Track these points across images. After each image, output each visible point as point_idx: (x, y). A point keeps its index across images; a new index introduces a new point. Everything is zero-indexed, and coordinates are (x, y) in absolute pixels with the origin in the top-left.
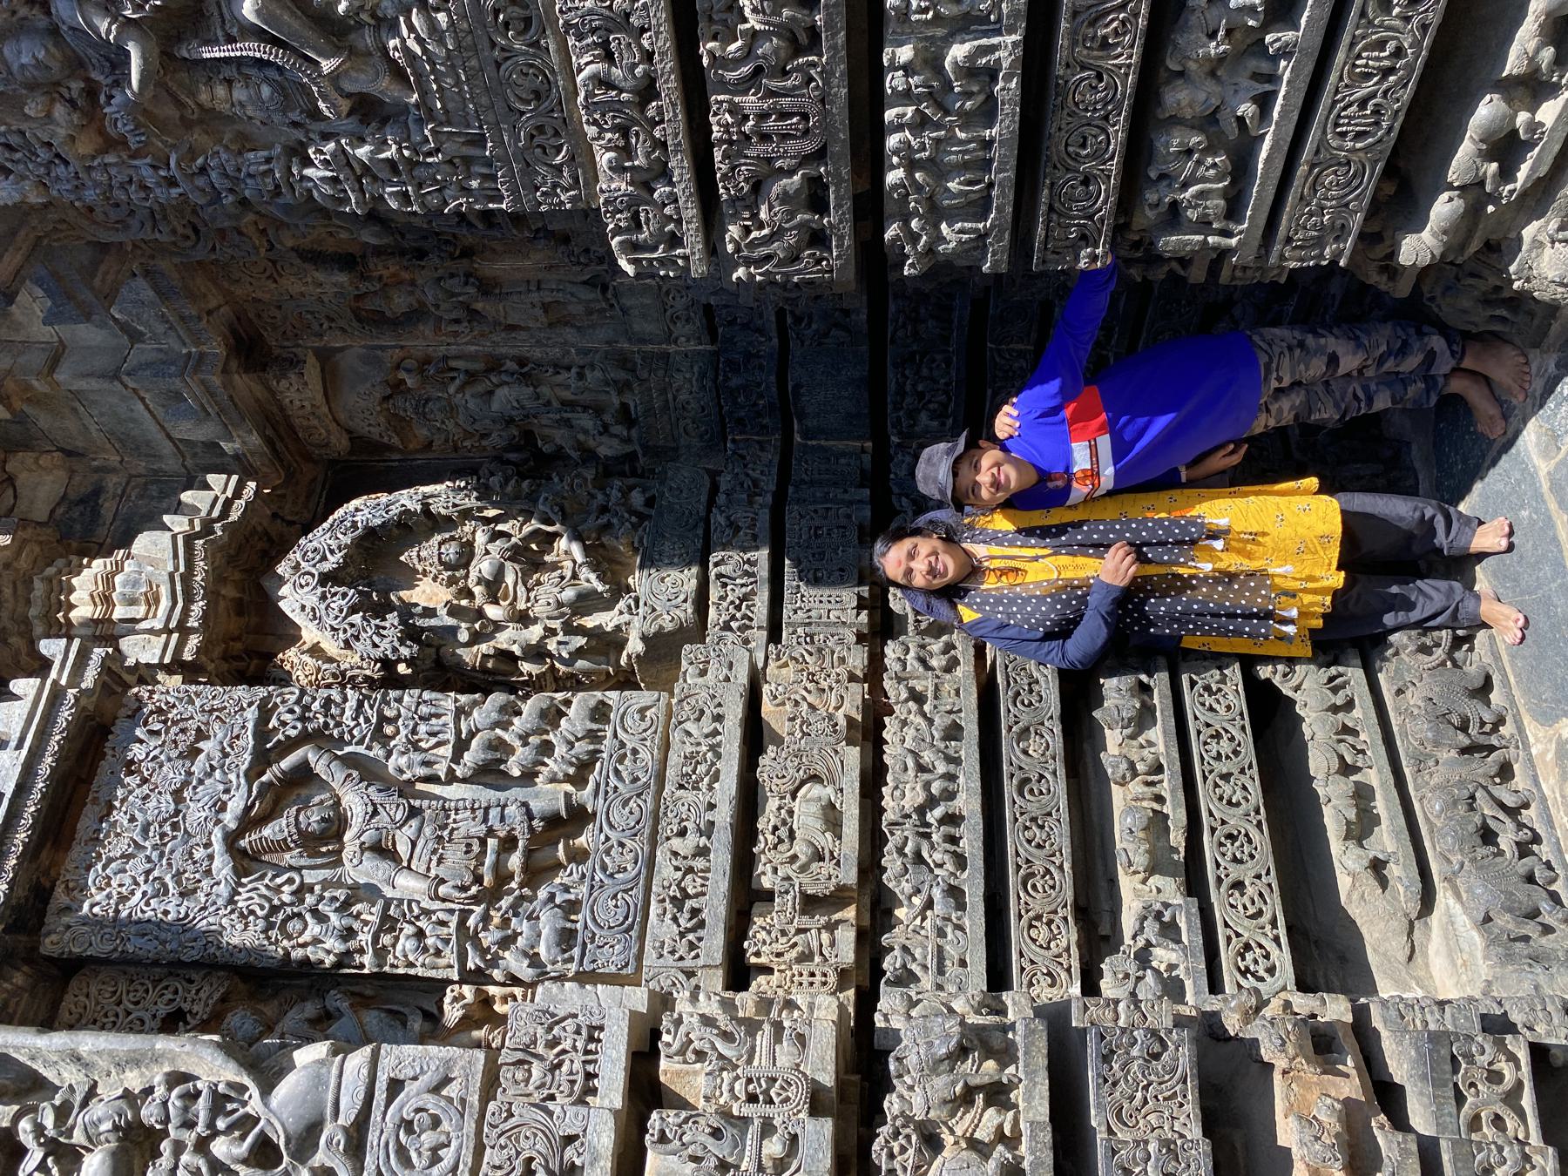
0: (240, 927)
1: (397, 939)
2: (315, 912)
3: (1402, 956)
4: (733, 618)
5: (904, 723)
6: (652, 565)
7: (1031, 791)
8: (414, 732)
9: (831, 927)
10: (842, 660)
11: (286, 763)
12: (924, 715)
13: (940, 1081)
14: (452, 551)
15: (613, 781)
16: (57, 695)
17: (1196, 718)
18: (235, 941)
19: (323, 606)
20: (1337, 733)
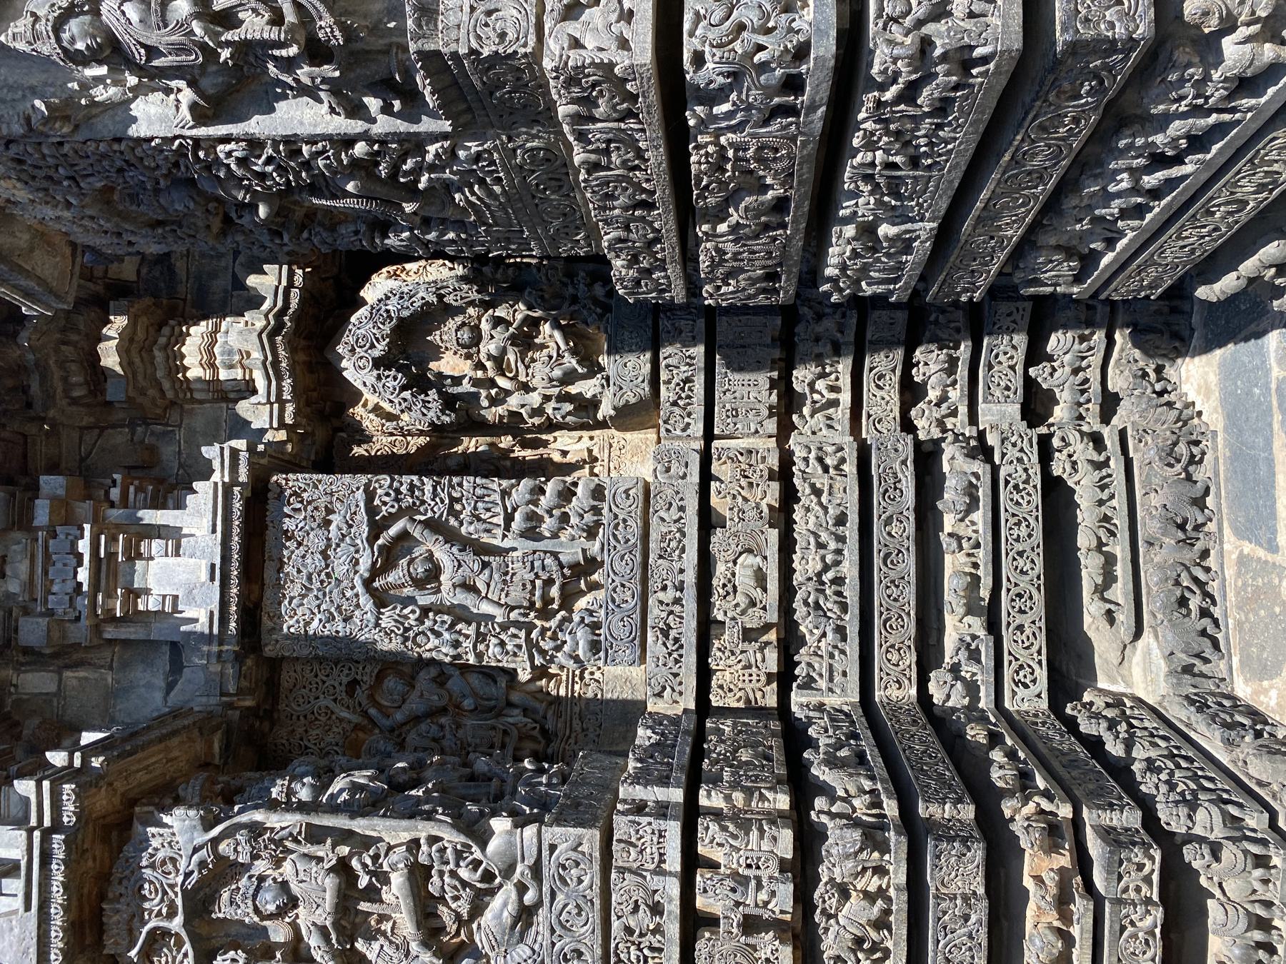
0: (387, 641)
1: (488, 646)
3: (1116, 662)
4: (680, 398)
5: (808, 510)
6: (617, 352)
7: (892, 562)
8: (475, 508)
9: (762, 649)
10: (764, 458)
11: (393, 531)
12: (820, 504)
13: (850, 864)
14: (465, 336)
15: (613, 541)
16: (228, 489)
17: (1006, 511)
18: (385, 649)
19: (380, 385)
20: (1100, 521)
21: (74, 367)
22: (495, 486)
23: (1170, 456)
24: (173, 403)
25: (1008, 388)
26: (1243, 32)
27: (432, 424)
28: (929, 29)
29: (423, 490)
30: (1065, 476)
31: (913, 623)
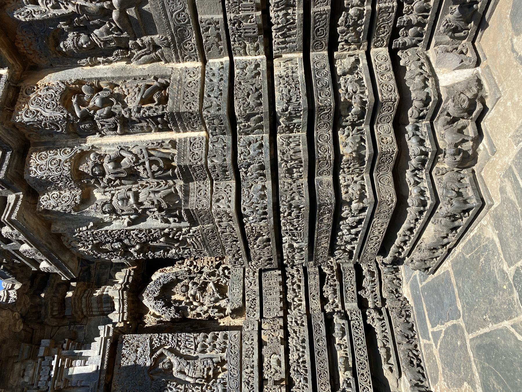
2: (170, 388)
4: (252, 305)
8: (185, 344)
9: (280, 388)
10: (278, 322)
12: (297, 336)
15: (230, 354)
21: (56, 305)
22: (192, 336)
23: (400, 315)
24: (85, 316)
25: (352, 298)
26: (355, 201)
27: (172, 318)
28: (291, 202)
29: (168, 338)
30: (371, 324)
31: (329, 375)
